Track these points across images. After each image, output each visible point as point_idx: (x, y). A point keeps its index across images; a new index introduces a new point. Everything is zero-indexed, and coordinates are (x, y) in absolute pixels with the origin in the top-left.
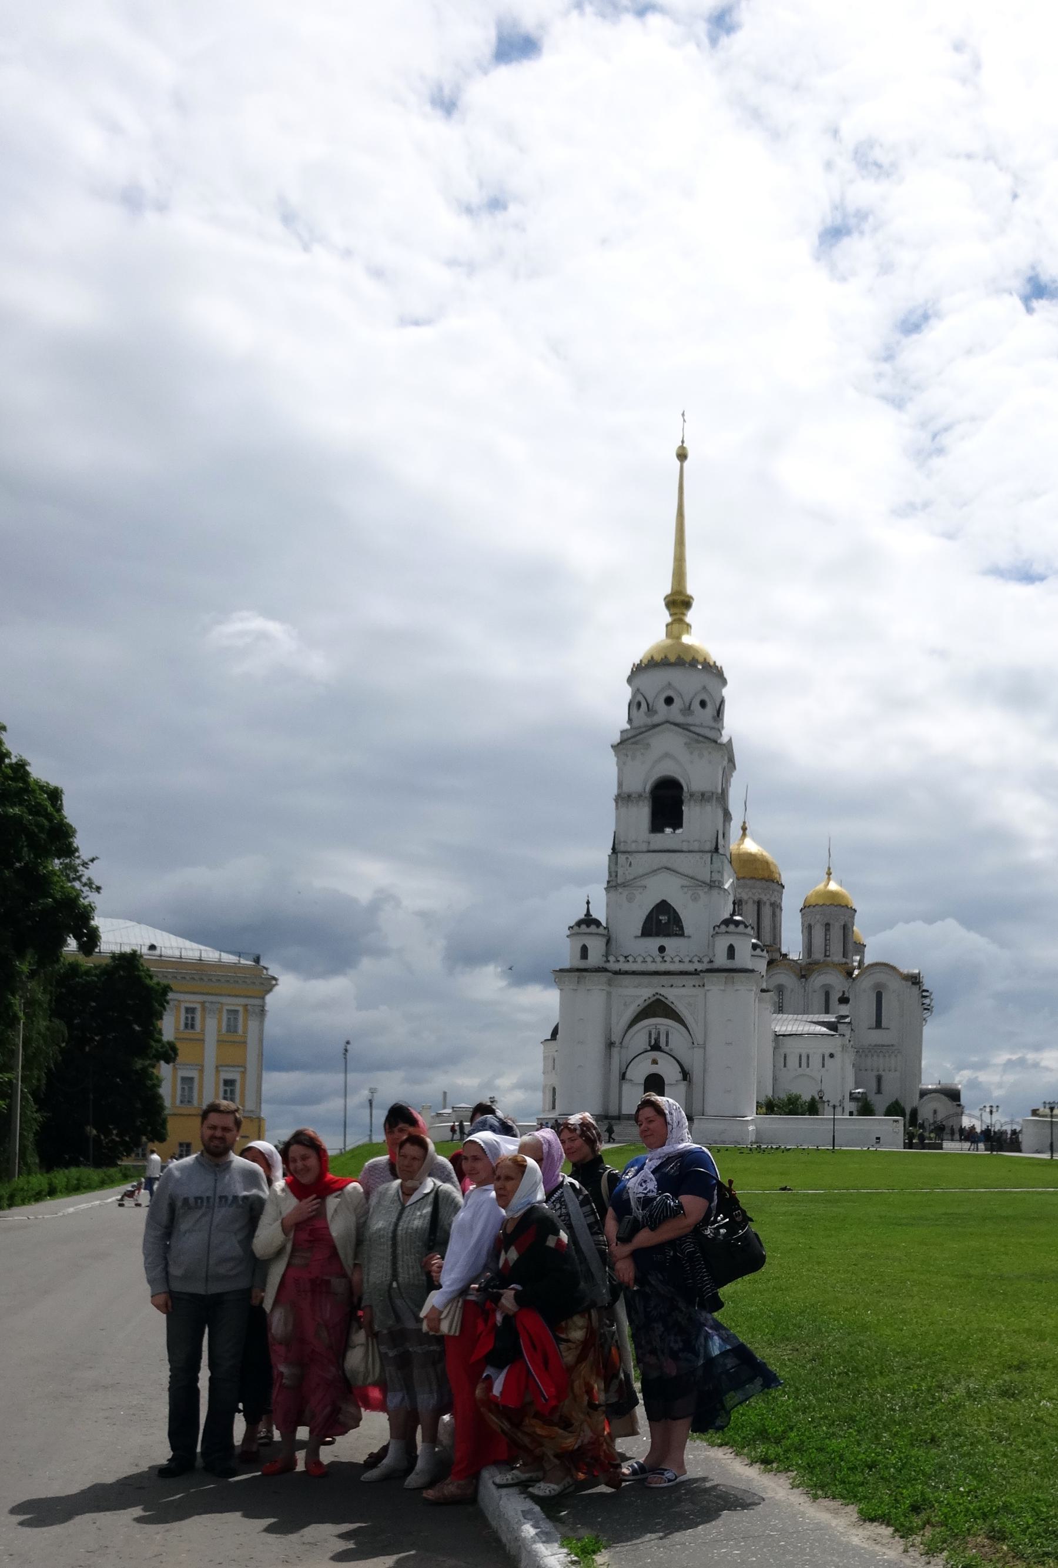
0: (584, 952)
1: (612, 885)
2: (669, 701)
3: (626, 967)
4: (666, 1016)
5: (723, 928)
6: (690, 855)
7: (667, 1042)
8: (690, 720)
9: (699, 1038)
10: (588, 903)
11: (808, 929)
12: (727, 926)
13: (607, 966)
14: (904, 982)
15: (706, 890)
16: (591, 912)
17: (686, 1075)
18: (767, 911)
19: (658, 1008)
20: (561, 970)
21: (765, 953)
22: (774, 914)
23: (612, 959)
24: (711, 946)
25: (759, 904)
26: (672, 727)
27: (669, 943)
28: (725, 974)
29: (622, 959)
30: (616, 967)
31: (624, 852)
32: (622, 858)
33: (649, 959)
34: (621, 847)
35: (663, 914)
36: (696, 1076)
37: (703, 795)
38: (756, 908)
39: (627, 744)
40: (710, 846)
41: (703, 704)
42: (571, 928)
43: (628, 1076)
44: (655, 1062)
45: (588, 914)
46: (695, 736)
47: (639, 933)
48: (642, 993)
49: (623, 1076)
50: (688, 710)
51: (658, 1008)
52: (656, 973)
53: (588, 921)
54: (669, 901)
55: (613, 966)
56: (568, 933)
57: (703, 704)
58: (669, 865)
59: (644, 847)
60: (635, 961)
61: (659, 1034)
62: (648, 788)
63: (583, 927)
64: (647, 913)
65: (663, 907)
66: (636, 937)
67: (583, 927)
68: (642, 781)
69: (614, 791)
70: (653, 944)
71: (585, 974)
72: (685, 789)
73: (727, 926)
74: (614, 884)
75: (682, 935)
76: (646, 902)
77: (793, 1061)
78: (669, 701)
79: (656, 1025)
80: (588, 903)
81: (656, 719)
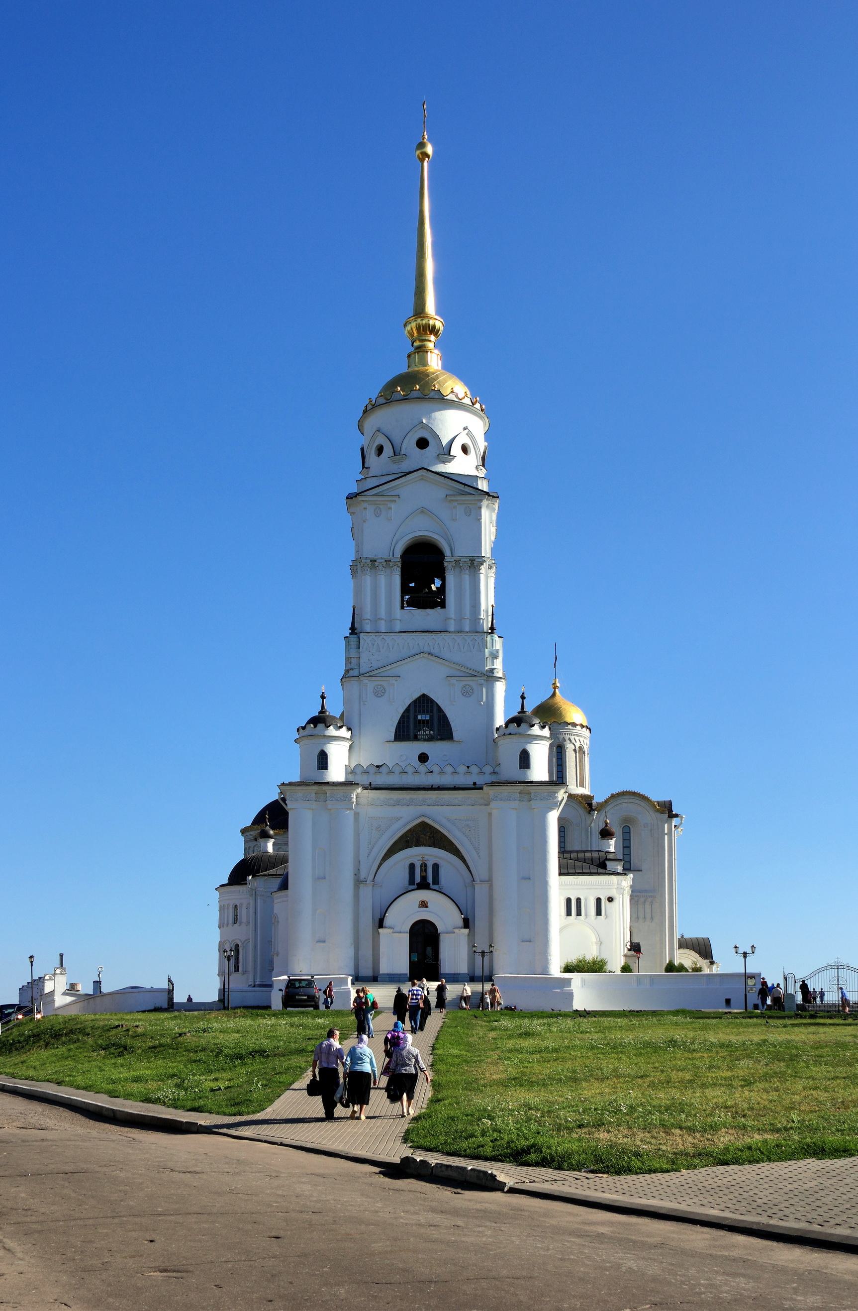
0: (323, 761)
4: (434, 845)
7: (436, 881)
9: (480, 871)
14: (658, 815)
19: (424, 834)
30: (365, 780)
33: (410, 770)
36: (480, 923)
44: (423, 904)
46: (461, 487)
47: (393, 738)
52: (432, 788)
54: (432, 696)
58: (426, 649)
60: (391, 772)
61: (424, 866)
62: (398, 552)
64: (401, 711)
65: (424, 703)
69: (351, 556)
72: (447, 553)
74: (356, 673)
78: (422, 443)
81: (405, 466)
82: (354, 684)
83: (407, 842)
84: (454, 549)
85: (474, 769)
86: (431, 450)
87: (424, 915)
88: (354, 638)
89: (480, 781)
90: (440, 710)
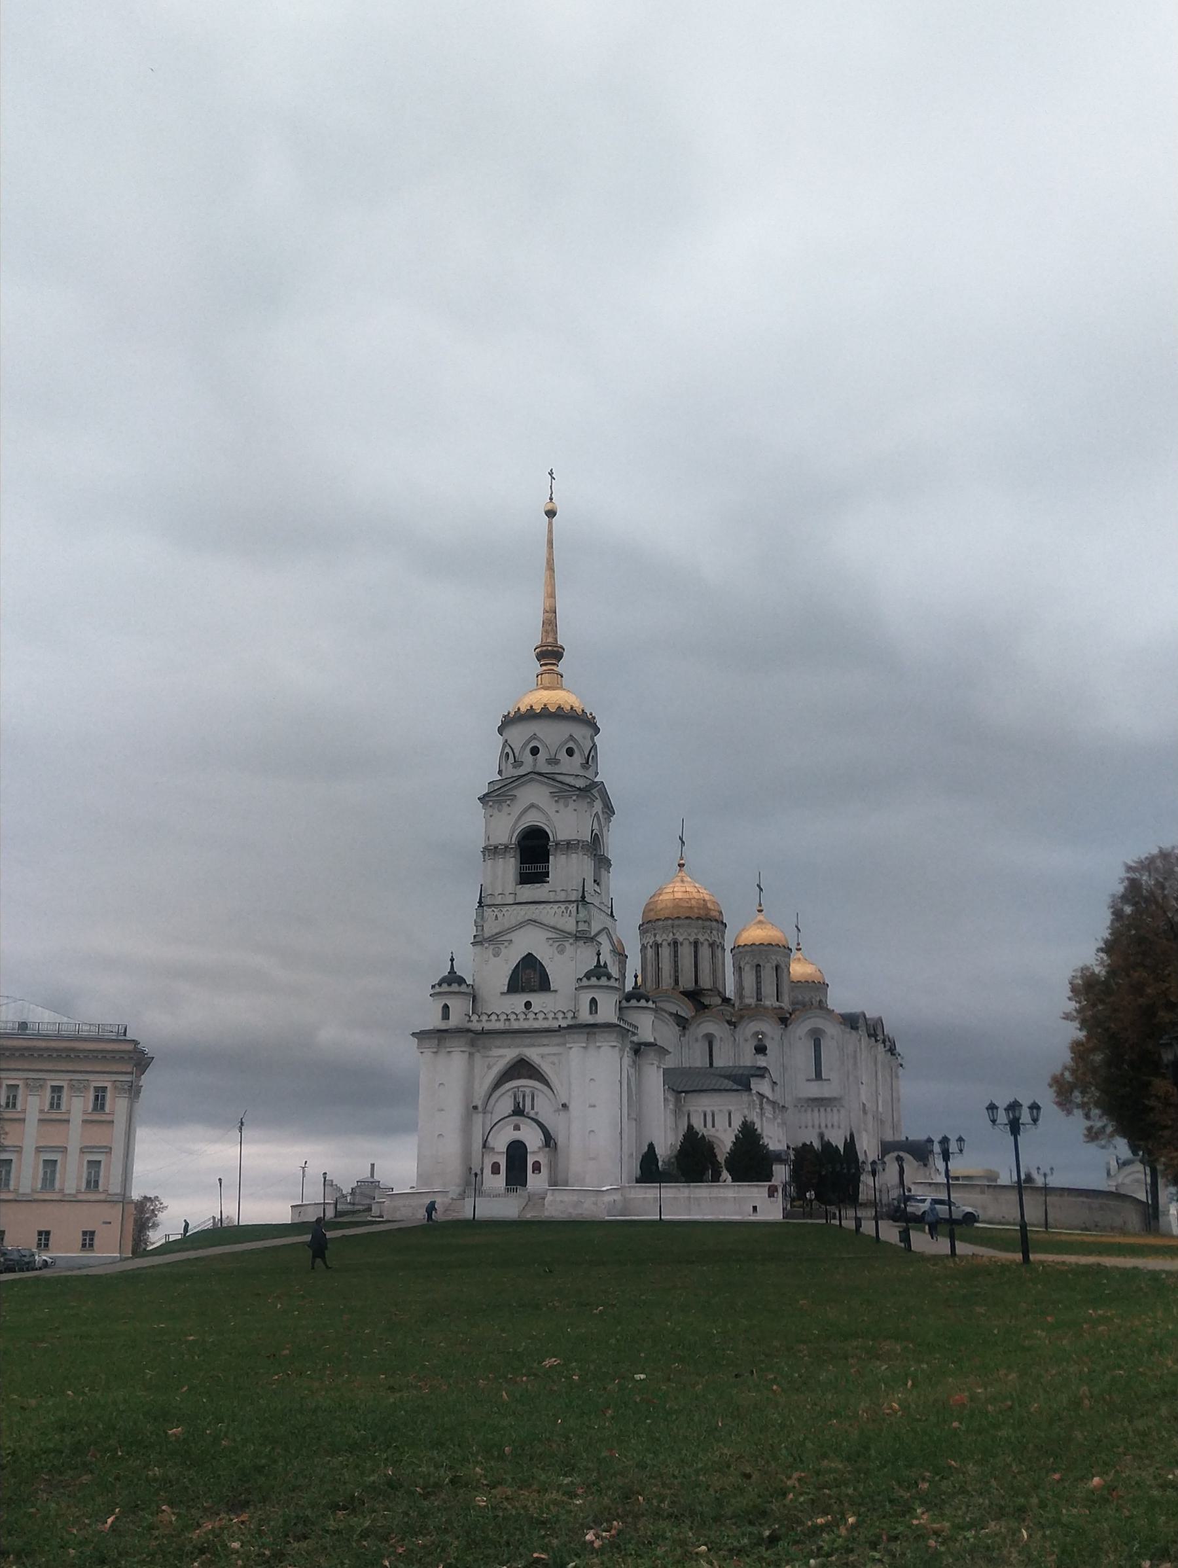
2: (535, 751)
3: (488, 1026)
4: (530, 1077)
5: (585, 982)
6: (556, 906)
7: (533, 1108)
8: (557, 769)
10: (452, 960)
11: (739, 970)
12: (589, 979)
13: (470, 1025)
15: (571, 941)
17: (549, 1140)
18: (705, 952)
20: (422, 1032)
21: (650, 1004)
24: (576, 999)
25: (696, 944)
29: (484, 1018)
31: (489, 906)
33: (512, 1017)
34: (488, 901)
36: (561, 1141)
37: (568, 843)
39: (496, 796)
41: (570, 752)
42: (433, 987)
44: (517, 1128)
48: (506, 1055)
50: (553, 761)
51: (522, 1068)
53: (453, 978)
55: (475, 1026)
58: (534, 917)
60: (498, 1020)
63: (445, 985)
65: (529, 961)
66: (502, 994)
70: (519, 1000)
71: (445, 1035)
73: (589, 979)
74: (478, 939)
76: (513, 956)
78: (535, 751)
79: (518, 1087)
80: (452, 960)
81: (521, 771)
82: (478, 948)
85: (560, 1015)
86: (542, 756)
87: (517, 1135)
88: (480, 910)
89: (564, 1024)
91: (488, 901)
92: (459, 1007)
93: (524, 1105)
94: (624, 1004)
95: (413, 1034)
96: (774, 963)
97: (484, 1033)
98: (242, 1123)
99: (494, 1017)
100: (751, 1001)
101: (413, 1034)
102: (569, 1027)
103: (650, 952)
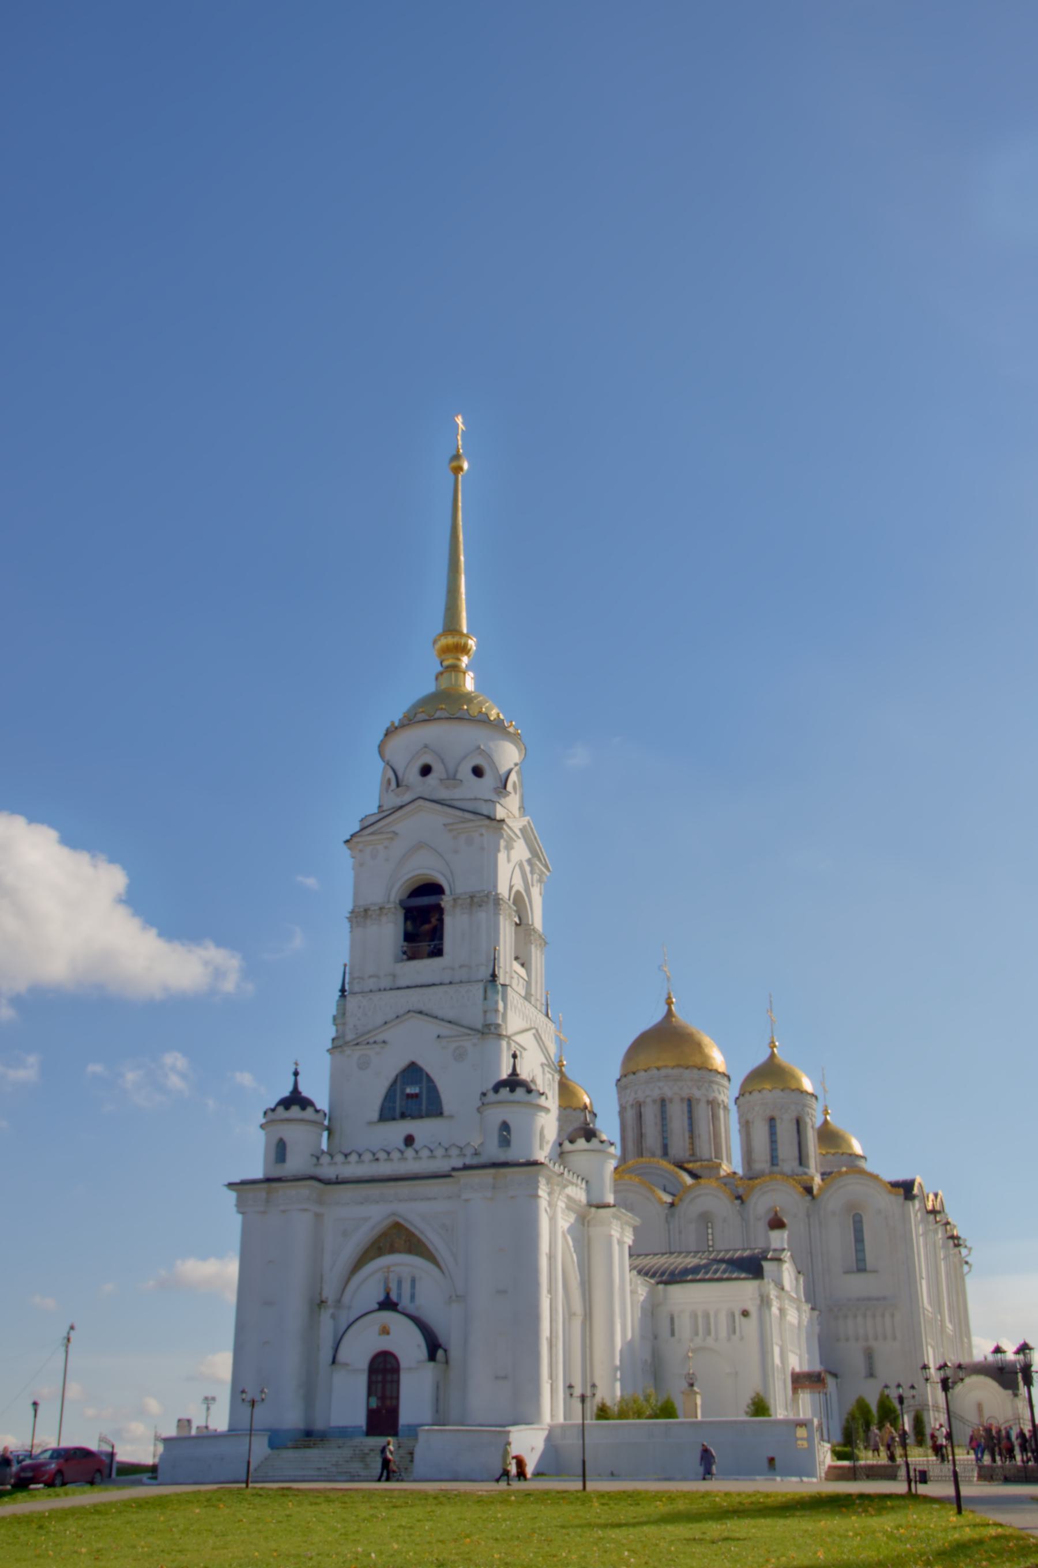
1: (338, 1045)
2: (426, 770)
5: (492, 1097)
10: (296, 1074)
16: (301, 1088)
19: (397, 1238)
20: (243, 1183)
22: (715, 1117)
23: (325, 1160)
26: (428, 804)
27: (422, 1129)
28: (492, 1171)
29: (339, 1158)
32: (352, 1002)
33: (382, 1156)
35: (413, 1083)
36: (455, 1353)
37: (472, 897)
38: (685, 1106)
40: (484, 973)
41: (478, 772)
43: (342, 1356)
45: (296, 1090)
47: (375, 1115)
49: (334, 1362)
50: (452, 779)
51: (397, 1238)
53: (295, 1100)
54: (421, 1063)
55: (328, 1171)
56: (263, 1121)
57: (478, 772)
59: (386, 982)
65: (413, 1072)
66: (370, 1123)
67: (281, 1109)
68: (389, 888)
69: (350, 907)
75: (440, 1114)
76: (387, 1066)
77: (684, 1325)
78: (426, 770)
79: (388, 1267)
80: (296, 1074)
83: (380, 1248)
84: (457, 885)
85: (454, 1152)
89: (459, 1164)
90: (430, 1080)
91: (356, 989)
92: (305, 1141)
93: (399, 1295)
94: (567, 1146)
95: (231, 1185)
96: (794, 1115)
97: (339, 1182)
98: (69, 1340)
99: (354, 1158)
100: (762, 1164)
101: (231, 1185)
102: (466, 1168)
103: (630, 1114)
